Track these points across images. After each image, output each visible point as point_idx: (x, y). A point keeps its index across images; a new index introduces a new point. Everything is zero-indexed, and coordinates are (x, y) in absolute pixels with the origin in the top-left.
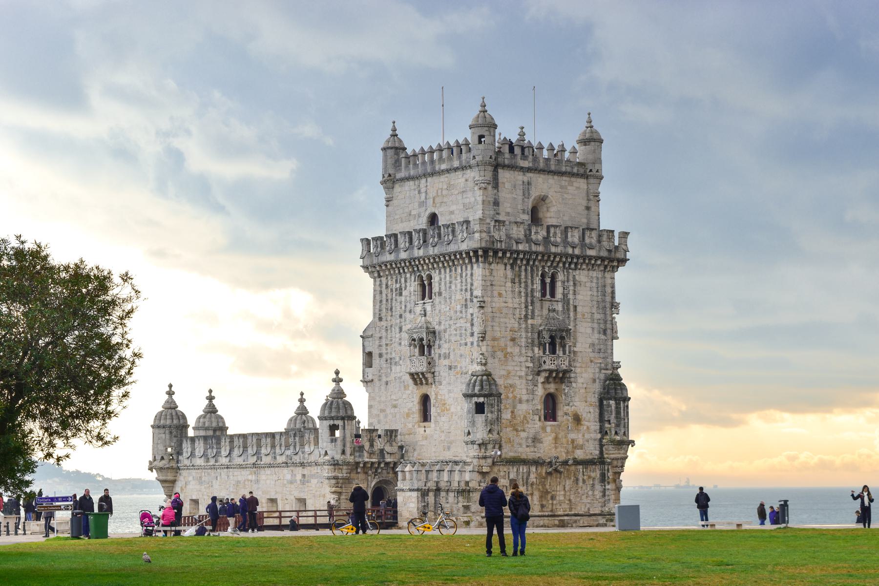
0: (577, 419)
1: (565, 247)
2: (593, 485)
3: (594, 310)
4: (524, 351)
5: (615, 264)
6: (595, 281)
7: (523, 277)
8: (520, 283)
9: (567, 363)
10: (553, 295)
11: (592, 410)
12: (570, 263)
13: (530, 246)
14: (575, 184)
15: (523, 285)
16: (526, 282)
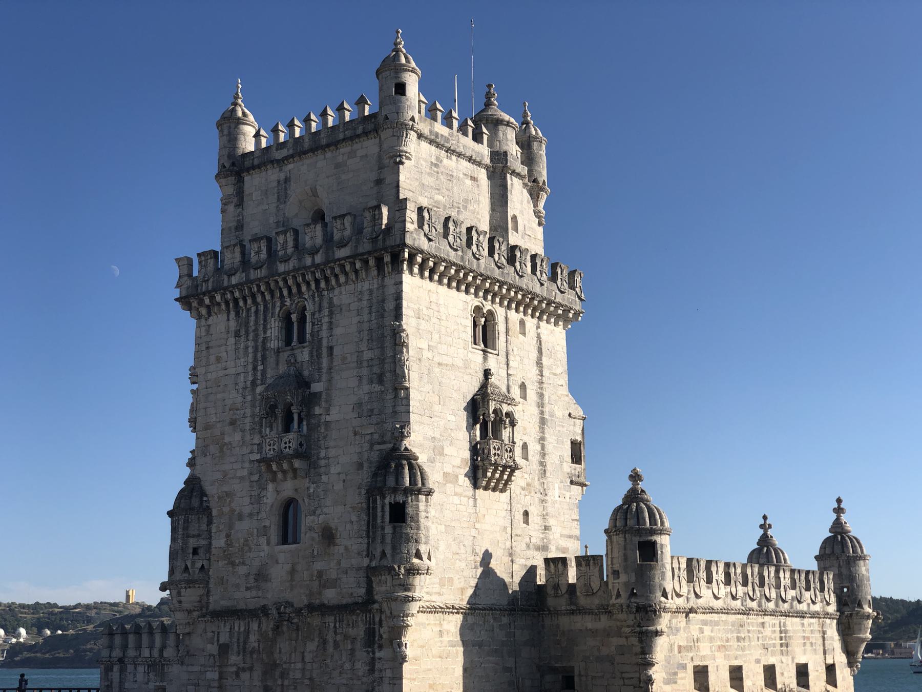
0: (328, 536)
1: (300, 259)
2: (353, 650)
3: (363, 346)
4: (248, 438)
5: (387, 258)
6: (366, 297)
7: (252, 323)
8: (247, 333)
9: (293, 445)
10: (302, 340)
11: (354, 518)
12: (317, 282)
13: (247, 276)
14: (360, 153)
15: (251, 337)
16: (256, 330)
